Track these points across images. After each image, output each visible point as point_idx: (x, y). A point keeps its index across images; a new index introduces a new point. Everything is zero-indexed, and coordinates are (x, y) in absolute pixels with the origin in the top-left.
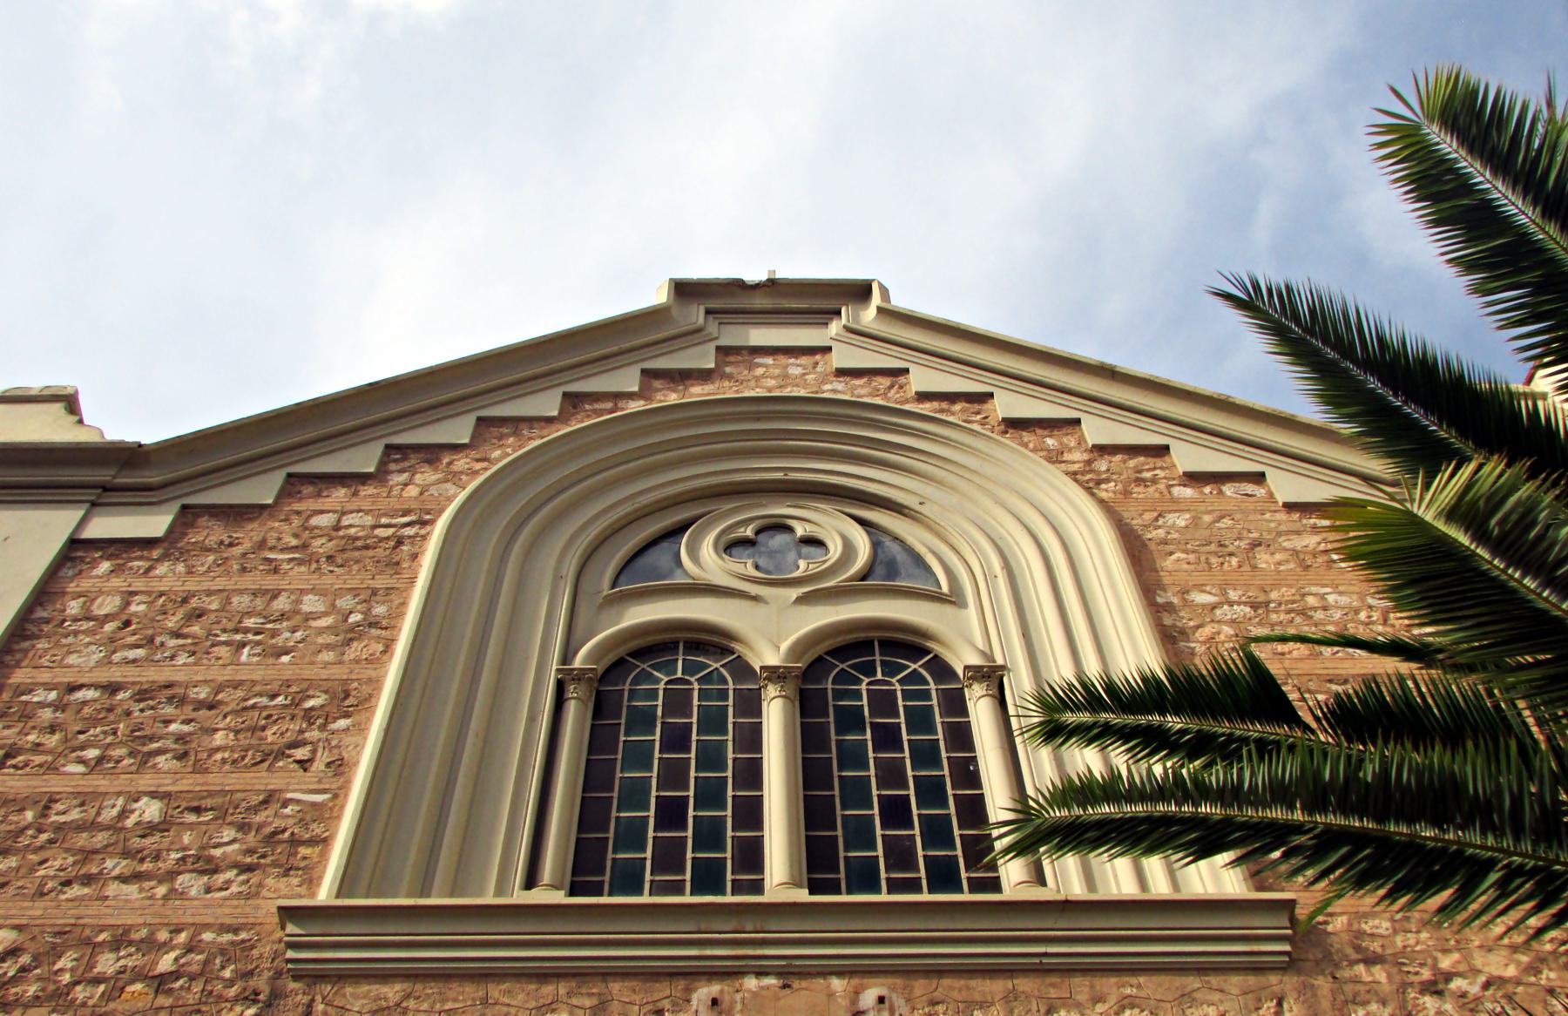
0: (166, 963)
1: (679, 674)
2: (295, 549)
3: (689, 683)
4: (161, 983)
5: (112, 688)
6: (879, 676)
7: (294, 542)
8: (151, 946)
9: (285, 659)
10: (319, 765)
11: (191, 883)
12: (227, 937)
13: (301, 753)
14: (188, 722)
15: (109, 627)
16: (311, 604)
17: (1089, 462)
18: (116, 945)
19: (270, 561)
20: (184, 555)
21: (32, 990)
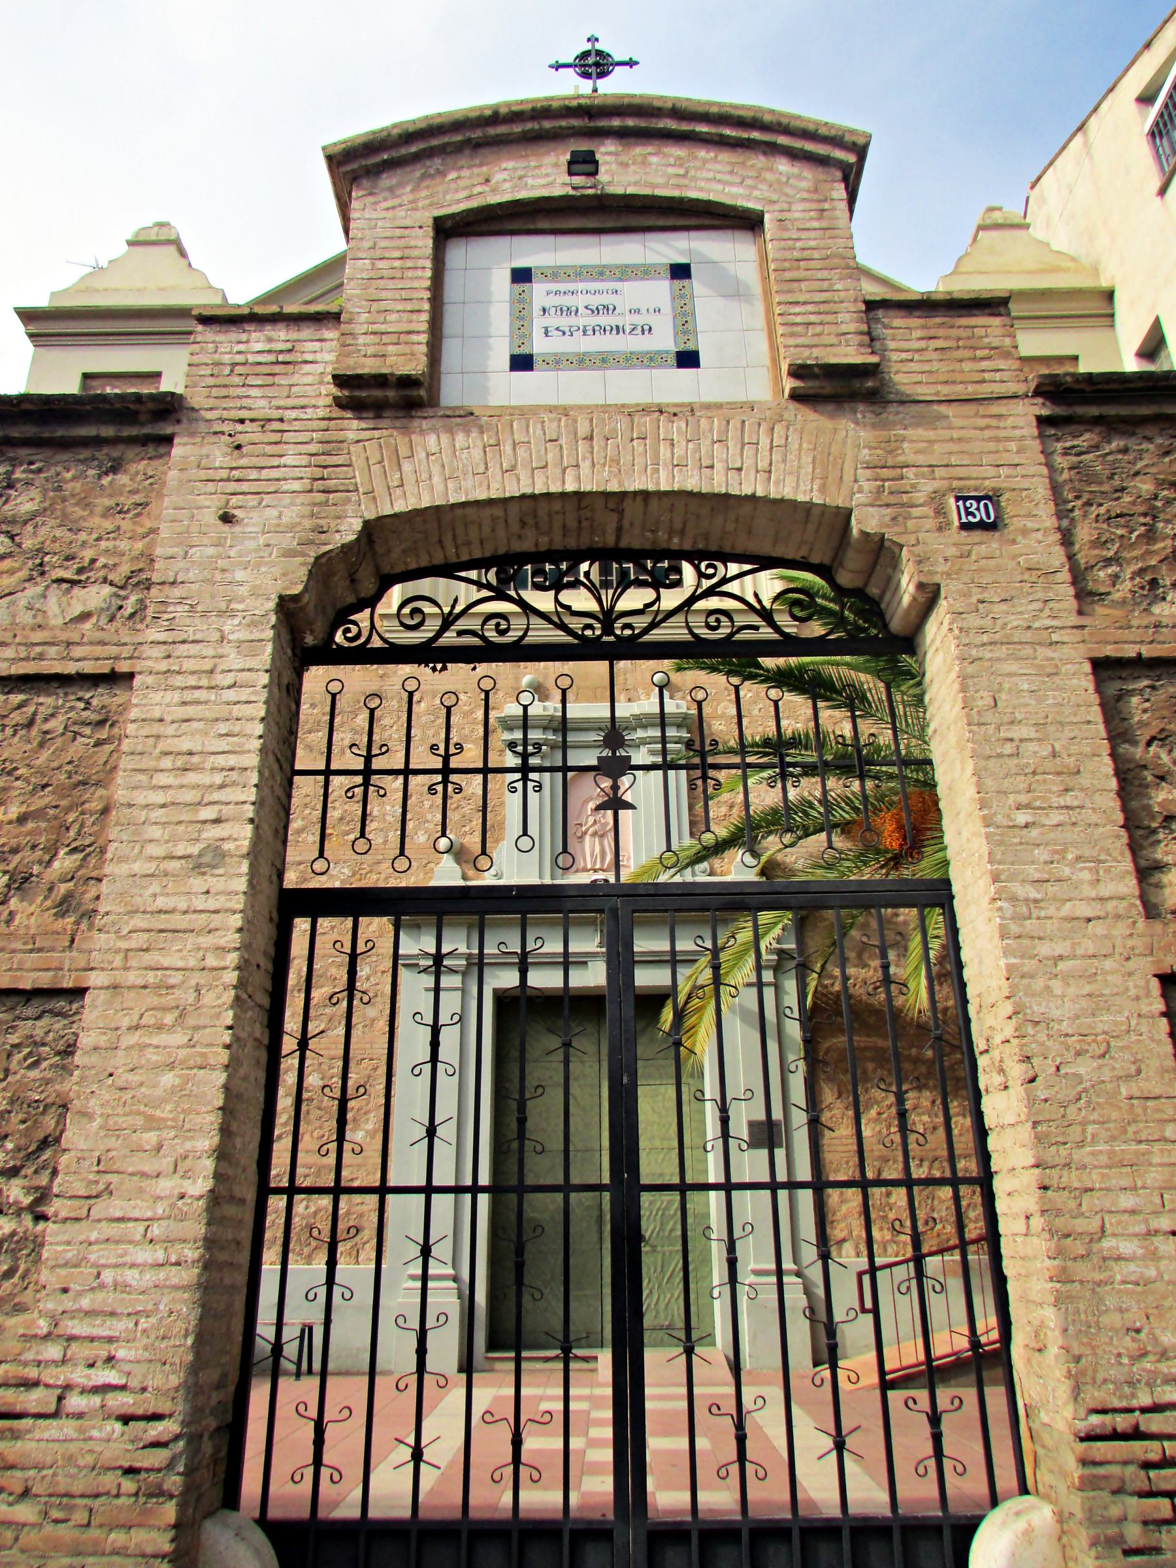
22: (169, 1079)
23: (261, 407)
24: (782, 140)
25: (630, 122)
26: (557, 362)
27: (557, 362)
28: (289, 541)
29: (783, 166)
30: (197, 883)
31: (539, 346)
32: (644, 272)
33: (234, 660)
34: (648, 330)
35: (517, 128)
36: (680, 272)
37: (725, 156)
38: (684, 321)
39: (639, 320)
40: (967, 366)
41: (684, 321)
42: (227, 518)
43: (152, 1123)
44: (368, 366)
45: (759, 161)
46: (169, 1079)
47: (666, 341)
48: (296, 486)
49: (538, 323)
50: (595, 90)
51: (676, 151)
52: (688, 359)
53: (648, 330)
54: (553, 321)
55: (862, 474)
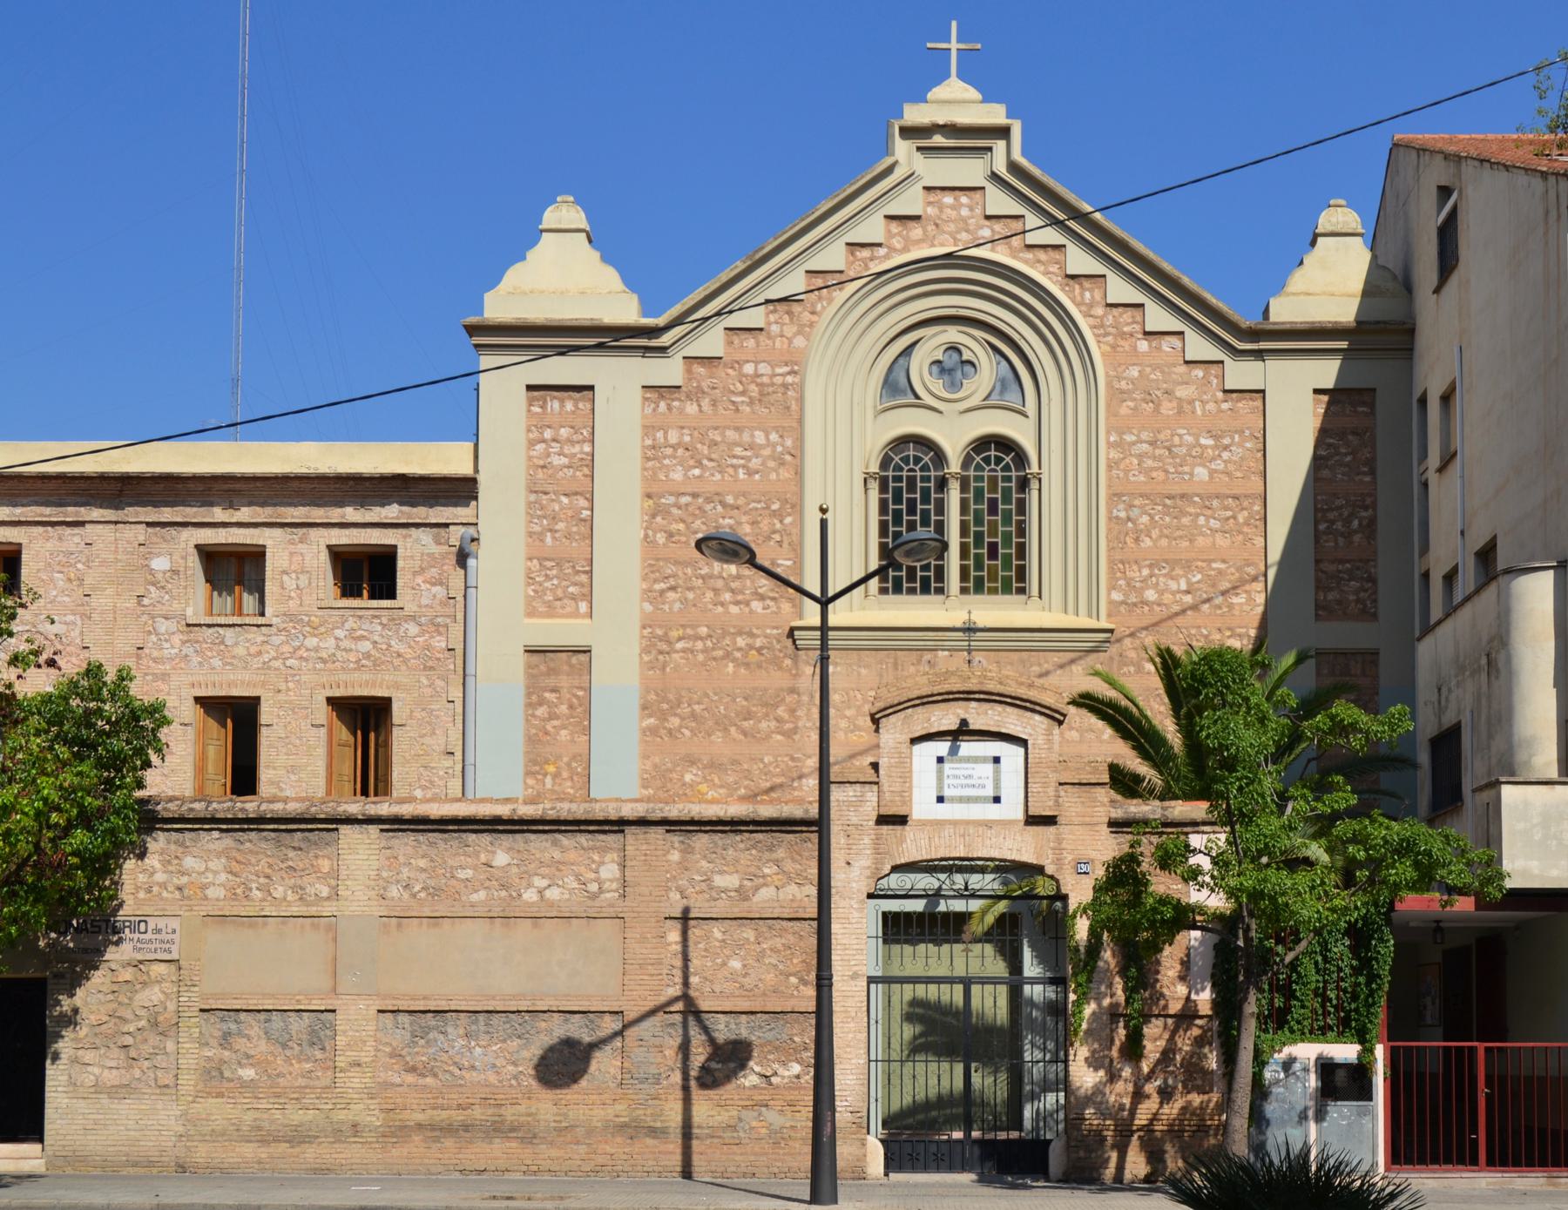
0: (758, 643)
1: (912, 466)
2: (743, 393)
3: (915, 471)
4: (759, 650)
5: (695, 495)
6: (993, 466)
7: (740, 388)
8: (751, 635)
9: (757, 477)
10: (785, 545)
11: (756, 605)
12: (775, 631)
13: (777, 537)
14: (731, 518)
15: (680, 452)
16: (760, 437)
17: (1102, 318)
18: (740, 633)
19: (733, 402)
20: (696, 395)
21: (720, 653)
22: (851, 1035)
23: (854, 820)
24: (1038, 708)
25: (982, 696)
26: (953, 800)
27: (953, 800)
28: (868, 873)
29: (1037, 717)
30: (853, 983)
31: (947, 793)
32: (984, 760)
33: (856, 914)
34: (984, 787)
35: (940, 698)
36: (997, 760)
37: (1016, 711)
38: (997, 785)
39: (980, 782)
40: (1089, 810)
41: (997, 785)
42: (849, 863)
43: (848, 1046)
44: (899, 827)
45: (1029, 714)
46: (851, 1035)
47: (990, 792)
48: (868, 852)
49: (947, 782)
50: (969, 612)
51: (999, 708)
52: (997, 800)
53: (984, 787)
54: (951, 781)
55: (1050, 852)
